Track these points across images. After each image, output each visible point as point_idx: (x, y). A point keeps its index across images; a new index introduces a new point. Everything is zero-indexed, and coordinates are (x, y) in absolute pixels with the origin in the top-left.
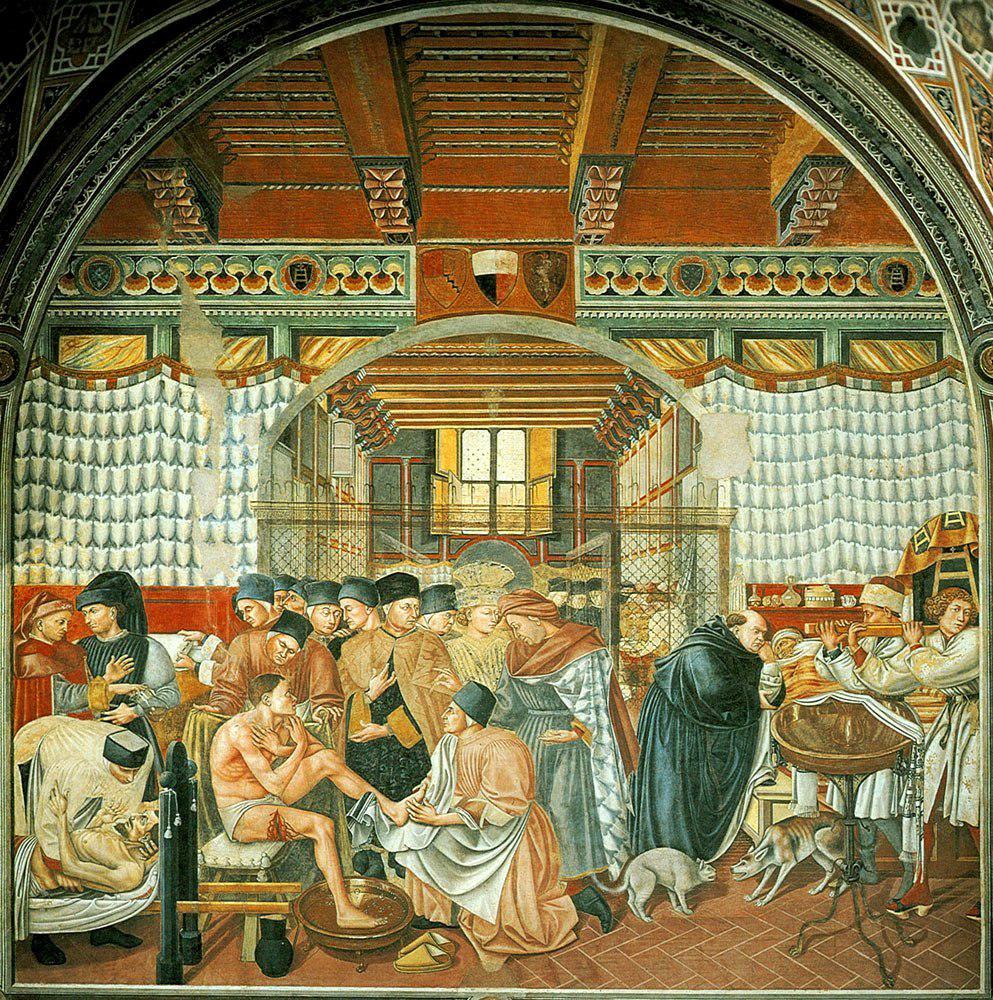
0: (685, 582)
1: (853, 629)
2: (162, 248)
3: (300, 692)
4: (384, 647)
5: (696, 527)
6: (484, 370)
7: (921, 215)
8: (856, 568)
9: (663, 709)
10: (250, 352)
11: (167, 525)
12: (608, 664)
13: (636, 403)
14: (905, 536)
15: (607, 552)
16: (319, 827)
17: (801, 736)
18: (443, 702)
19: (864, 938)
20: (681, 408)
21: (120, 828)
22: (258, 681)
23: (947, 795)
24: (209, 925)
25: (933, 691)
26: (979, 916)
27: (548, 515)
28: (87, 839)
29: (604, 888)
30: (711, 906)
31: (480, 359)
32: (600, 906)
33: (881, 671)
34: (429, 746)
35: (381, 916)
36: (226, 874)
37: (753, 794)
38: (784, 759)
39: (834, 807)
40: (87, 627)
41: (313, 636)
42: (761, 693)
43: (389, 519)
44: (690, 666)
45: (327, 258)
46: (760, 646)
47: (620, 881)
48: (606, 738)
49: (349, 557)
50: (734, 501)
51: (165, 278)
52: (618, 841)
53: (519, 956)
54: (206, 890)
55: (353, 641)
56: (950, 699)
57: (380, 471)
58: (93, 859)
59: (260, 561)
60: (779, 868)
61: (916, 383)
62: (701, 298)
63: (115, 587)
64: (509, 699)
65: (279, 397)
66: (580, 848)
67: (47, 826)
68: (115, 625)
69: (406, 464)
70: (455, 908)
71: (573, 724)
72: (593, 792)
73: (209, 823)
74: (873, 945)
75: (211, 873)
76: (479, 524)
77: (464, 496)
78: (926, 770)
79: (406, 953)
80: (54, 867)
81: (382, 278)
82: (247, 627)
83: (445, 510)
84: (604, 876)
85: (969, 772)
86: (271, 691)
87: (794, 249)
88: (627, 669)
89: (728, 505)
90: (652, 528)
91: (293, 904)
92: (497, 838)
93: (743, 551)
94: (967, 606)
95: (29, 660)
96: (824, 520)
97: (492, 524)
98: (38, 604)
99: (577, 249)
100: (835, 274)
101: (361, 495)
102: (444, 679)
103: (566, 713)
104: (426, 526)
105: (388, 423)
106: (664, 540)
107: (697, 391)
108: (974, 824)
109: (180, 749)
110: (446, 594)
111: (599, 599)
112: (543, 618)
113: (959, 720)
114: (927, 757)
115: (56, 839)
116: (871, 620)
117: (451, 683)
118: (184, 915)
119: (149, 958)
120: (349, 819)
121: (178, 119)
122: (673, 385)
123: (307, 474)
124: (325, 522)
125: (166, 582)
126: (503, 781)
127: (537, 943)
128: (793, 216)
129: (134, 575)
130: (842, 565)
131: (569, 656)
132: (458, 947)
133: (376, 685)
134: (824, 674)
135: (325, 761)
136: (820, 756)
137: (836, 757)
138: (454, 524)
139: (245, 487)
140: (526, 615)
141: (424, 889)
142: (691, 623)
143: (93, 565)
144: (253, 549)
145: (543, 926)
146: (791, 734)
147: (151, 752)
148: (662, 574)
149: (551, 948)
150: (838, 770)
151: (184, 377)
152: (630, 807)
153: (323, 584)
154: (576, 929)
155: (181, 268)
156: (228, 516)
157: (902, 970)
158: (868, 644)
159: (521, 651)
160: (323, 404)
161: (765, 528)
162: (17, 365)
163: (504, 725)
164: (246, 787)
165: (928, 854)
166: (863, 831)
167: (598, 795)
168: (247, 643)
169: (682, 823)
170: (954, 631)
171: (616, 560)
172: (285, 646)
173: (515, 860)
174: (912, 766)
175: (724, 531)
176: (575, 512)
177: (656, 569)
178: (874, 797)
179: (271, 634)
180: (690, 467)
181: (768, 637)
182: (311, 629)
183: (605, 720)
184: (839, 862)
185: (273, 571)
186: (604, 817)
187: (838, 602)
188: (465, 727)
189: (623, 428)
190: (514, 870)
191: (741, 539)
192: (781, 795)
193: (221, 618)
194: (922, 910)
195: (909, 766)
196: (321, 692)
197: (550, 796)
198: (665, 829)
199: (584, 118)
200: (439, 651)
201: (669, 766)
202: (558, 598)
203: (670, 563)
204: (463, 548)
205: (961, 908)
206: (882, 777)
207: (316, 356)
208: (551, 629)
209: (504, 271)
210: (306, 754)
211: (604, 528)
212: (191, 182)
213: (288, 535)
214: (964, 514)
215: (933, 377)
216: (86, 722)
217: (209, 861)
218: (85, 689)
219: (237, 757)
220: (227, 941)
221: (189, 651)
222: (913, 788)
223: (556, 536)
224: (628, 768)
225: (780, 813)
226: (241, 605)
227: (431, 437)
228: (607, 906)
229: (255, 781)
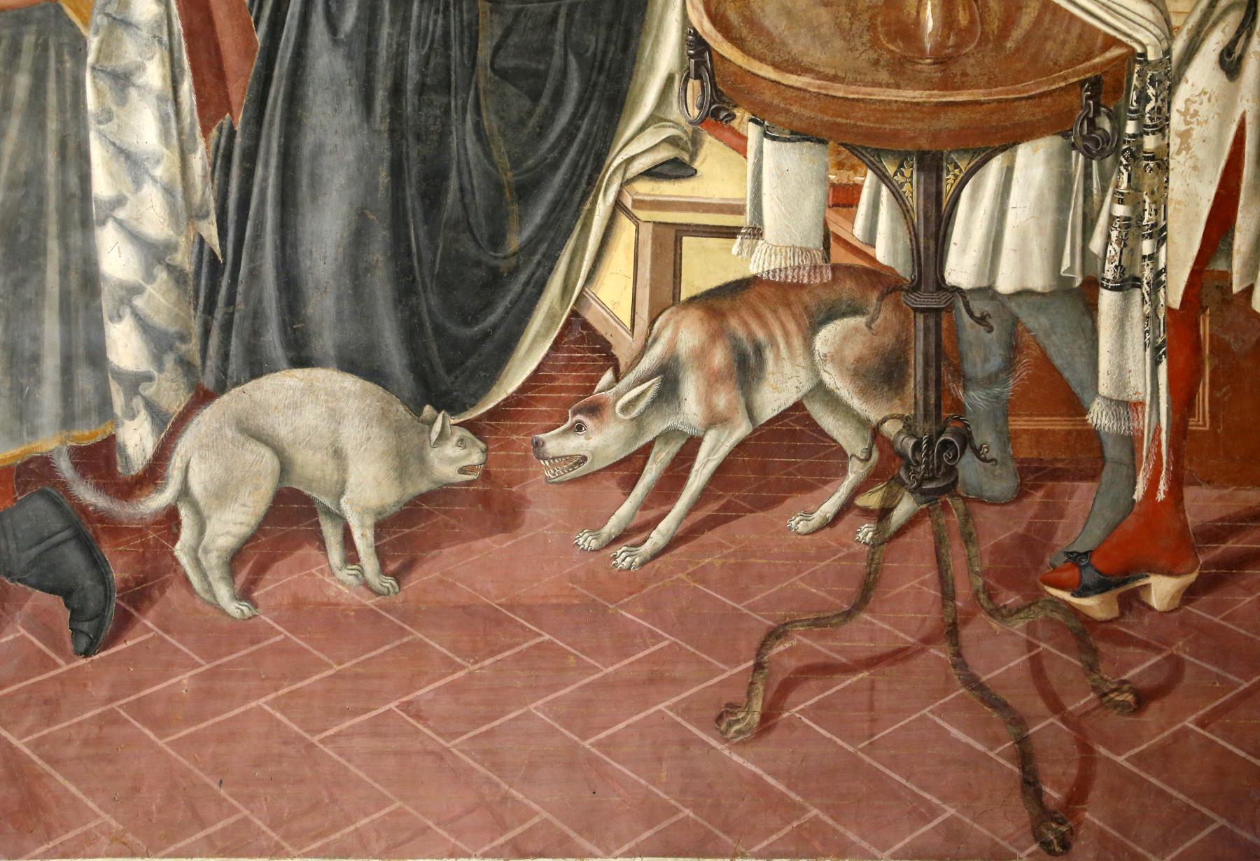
19: (973, 683)
29: (89, 495)
30: (468, 567)
32: (74, 558)
37: (618, 205)
38: (721, 97)
39: (882, 253)
47: (154, 473)
52: (159, 342)
60: (691, 446)
72: (85, 179)
74: (999, 705)
78: (1175, 143)
84: (99, 459)
114: (1178, 103)
136: (839, 91)
137: (891, 95)
146: (752, 23)
150: (895, 135)
152: (210, 230)
157: (1095, 794)
165: (1183, 402)
167: (102, 187)
174: (1131, 128)
178: (1007, 224)
186: (116, 259)
194: (1161, 590)
195: (1119, 128)
198: (323, 306)
201: (349, 103)
206: (1033, 163)
222: (1132, 197)
224: (212, 102)
228: (98, 564)
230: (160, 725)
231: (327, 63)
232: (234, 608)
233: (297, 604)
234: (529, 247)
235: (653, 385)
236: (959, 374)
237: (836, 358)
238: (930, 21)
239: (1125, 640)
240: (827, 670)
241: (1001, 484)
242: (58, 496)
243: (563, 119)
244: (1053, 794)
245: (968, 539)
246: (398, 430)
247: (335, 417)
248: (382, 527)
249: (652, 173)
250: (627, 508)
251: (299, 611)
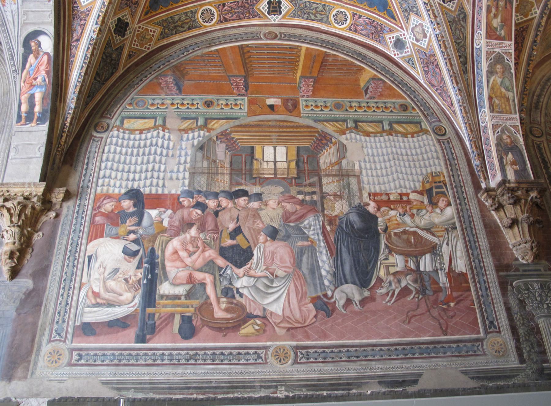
0: (346, 191)
1: (408, 207)
2: (163, 96)
3: (202, 229)
4: (235, 213)
5: (348, 176)
6: (271, 129)
7: (408, 93)
8: (405, 187)
9: (343, 234)
10: (190, 124)
11: (156, 174)
12: (321, 219)
13: (323, 140)
14: (421, 178)
15: (317, 183)
16: (208, 279)
17: (395, 242)
18: (258, 232)
19: (433, 316)
20: (339, 141)
21: (126, 280)
22: (187, 225)
23: (453, 262)
24: (160, 318)
25: (440, 227)
26: (474, 305)
27: (295, 172)
28: (112, 284)
30: (371, 306)
31: (269, 126)
32: (325, 307)
33: (421, 221)
34: (253, 248)
35: (233, 313)
36: (168, 297)
38: (390, 251)
39: (412, 267)
40: (121, 207)
41: (208, 210)
42: (379, 228)
43: (237, 172)
44: (351, 219)
45: (218, 100)
46: (376, 212)
47: (332, 297)
48: (322, 244)
49: (223, 183)
50: (360, 167)
51: (163, 104)
52: (330, 282)
53: (292, 328)
54: (159, 304)
55: (223, 211)
56: (447, 229)
57: (234, 158)
58: (113, 292)
59: (189, 185)
60: (394, 291)
61: (415, 135)
62: (342, 112)
63: (135, 195)
64: (284, 231)
65: (199, 136)
66: (315, 285)
67: (96, 279)
68: (132, 206)
69: (244, 156)
70: (264, 309)
71: (309, 239)
73: (163, 277)
74: (436, 319)
75: (162, 297)
76: (270, 174)
77: (265, 165)
79: (244, 328)
80: (96, 295)
81: (236, 105)
82: (183, 207)
83: (258, 170)
84: (326, 295)
85: (459, 254)
86: (190, 228)
87: (370, 100)
88: (328, 220)
89: (359, 169)
90: (333, 176)
91: (196, 308)
92: (281, 281)
93: (366, 182)
94: (446, 199)
95: (97, 219)
96: (392, 173)
97: (275, 174)
98: (104, 199)
99: (300, 99)
100: (384, 106)
101: (227, 165)
102: (258, 224)
103: (306, 236)
104: (251, 175)
105: (238, 144)
106: (337, 179)
107: (344, 136)
108: (464, 271)
109: (153, 251)
110: (258, 196)
111: (315, 197)
112: (295, 204)
113: (452, 236)
115: (98, 284)
116: (414, 204)
117: (261, 225)
118: (149, 314)
119: (132, 332)
120: (220, 275)
121: (171, 65)
122: (336, 135)
123: (208, 158)
124: (214, 173)
125: (154, 192)
126: (282, 260)
127: (299, 323)
128: (369, 91)
129: (142, 190)
130: (401, 187)
131: (306, 216)
132: (266, 325)
133: (232, 226)
134: (401, 221)
135: (211, 253)
138: (261, 174)
139: (185, 162)
140: (289, 203)
141: (251, 303)
142: (350, 205)
143: (127, 186)
144: (187, 182)
145: (302, 316)
147: (141, 252)
148: (338, 190)
149: (306, 324)
151: (166, 131)
152: (334, 269)
153: (212, 193)
154: (315, 316)
155: (169, 102)
156: (178, 171)
158: (414, 211)
159: (288, 214)
160: (215, 139)
161: (372, 176)
162: (108, 127)
163: (282, 240)
164: (178, 264)
165: (450, 283)
166: (424, 276)
167: (321, 265)
168: (183, 212)
169: (354, 274)
170: (444, 207)
171: (321, 185)
172: (197, 213)
173: (289, 290)
175: (358, 177)
176: (305, 170)
177: (336, 188)
178: (426, 263)
179: (191, 209)
180: (344, 157)
181: (379, 209)
182: (207, 207)
183: (321, 238)
184: (417, 287)
185: (194, 189)
186: (324, 273)
187: (401, 198)
188: (267, 241)
189: (320, 146)
190: (288, 294)
191: (365, 179)
192: (391, 264)
193: (173, 204)
194: (452, 304)
196: (210, 229)
197: (302, 266)
198: (348, 277)
199: (301, 67)
200: (256, 215)
201: (347, 254)
202: (300, 197)
203: (340, 186)
204: (263, 181)
205: (467, 303)
206: (428, 256)
207: (214, 125)
208: (298, 207)
209: (277, 104)
210: (203, 251)
211: (316, 175)
212: (174, 80)
213: (200, 177)
214: (439, 172)
215: (421, 134)
216: (117, 240)
217: (162, 292)
218: (118, 228)
219: (176, 252)
220: (166, 325)
221: (160, 215)
222: (440, 260)
223: (299, 177)
224: (332, 254)
225: (392, 270)
226: (181, 200)
227: (253, 148)
228: (328, 308)
229: (182, 261)
230: (338, 326)
231: (344, 249)
232: (344, 312)
233: (351, 311)
234: (371, 269)
235: (388, 284)
236: (424, 281)
237: (409, 280)
238: (413, 241)
239: (449, 310)
240: (415, 316)
241: (431, 293)
242: (322, 300)
243: (372, 254)
244: (444, 329)
245: (429, 300)
246: (360, 291)
247: (352, 290)
248: (360, 302)
249: (384, 260)
250: (388, 299)
251: (352, 312)
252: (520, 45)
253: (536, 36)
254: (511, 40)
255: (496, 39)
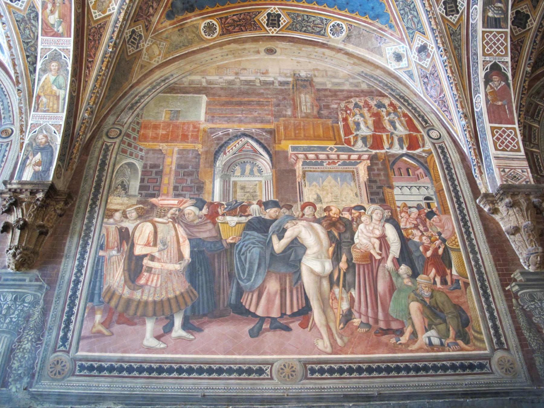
252: (97, 42)
253: (114, 31)
254: (70, 37)
255: (53, 36)
